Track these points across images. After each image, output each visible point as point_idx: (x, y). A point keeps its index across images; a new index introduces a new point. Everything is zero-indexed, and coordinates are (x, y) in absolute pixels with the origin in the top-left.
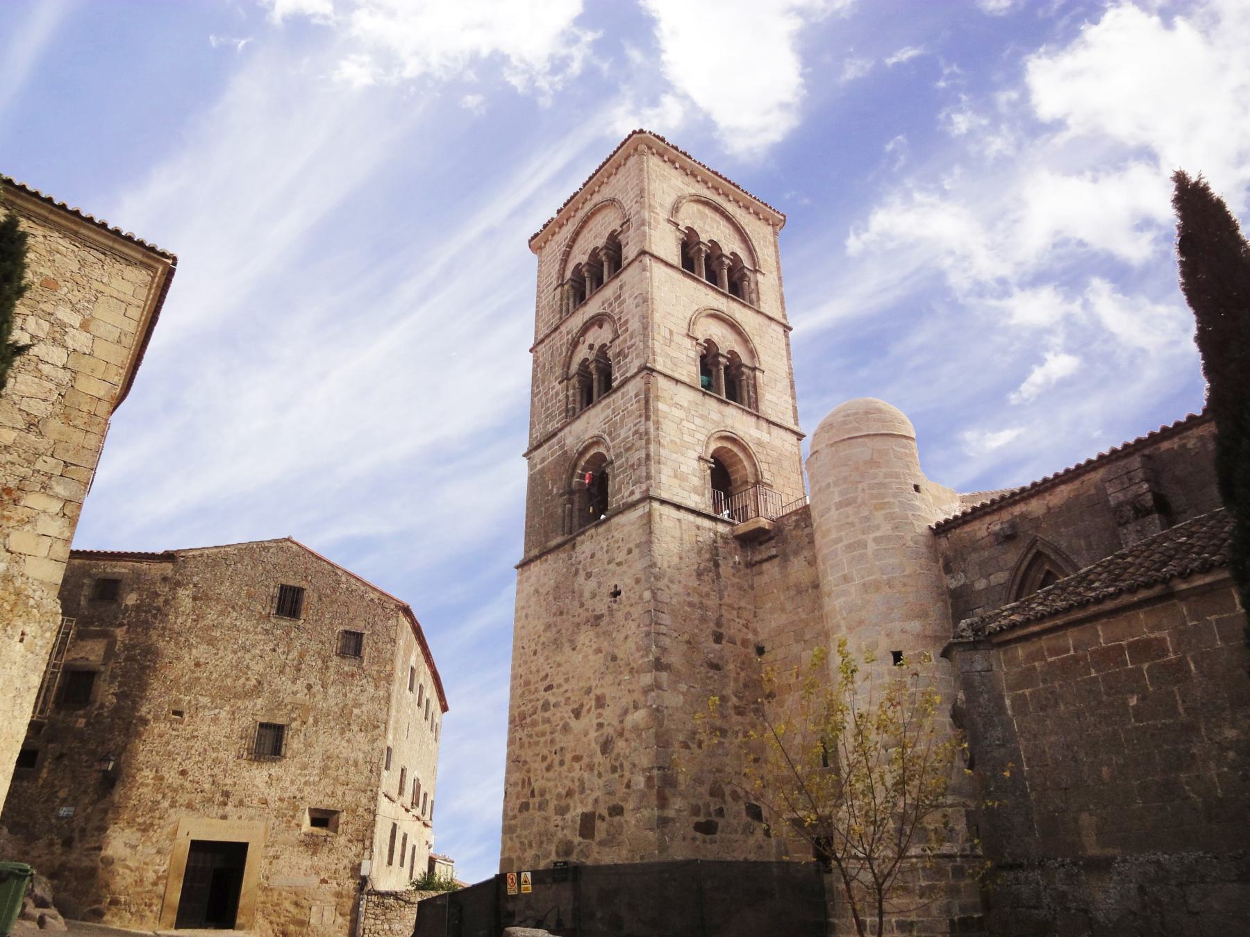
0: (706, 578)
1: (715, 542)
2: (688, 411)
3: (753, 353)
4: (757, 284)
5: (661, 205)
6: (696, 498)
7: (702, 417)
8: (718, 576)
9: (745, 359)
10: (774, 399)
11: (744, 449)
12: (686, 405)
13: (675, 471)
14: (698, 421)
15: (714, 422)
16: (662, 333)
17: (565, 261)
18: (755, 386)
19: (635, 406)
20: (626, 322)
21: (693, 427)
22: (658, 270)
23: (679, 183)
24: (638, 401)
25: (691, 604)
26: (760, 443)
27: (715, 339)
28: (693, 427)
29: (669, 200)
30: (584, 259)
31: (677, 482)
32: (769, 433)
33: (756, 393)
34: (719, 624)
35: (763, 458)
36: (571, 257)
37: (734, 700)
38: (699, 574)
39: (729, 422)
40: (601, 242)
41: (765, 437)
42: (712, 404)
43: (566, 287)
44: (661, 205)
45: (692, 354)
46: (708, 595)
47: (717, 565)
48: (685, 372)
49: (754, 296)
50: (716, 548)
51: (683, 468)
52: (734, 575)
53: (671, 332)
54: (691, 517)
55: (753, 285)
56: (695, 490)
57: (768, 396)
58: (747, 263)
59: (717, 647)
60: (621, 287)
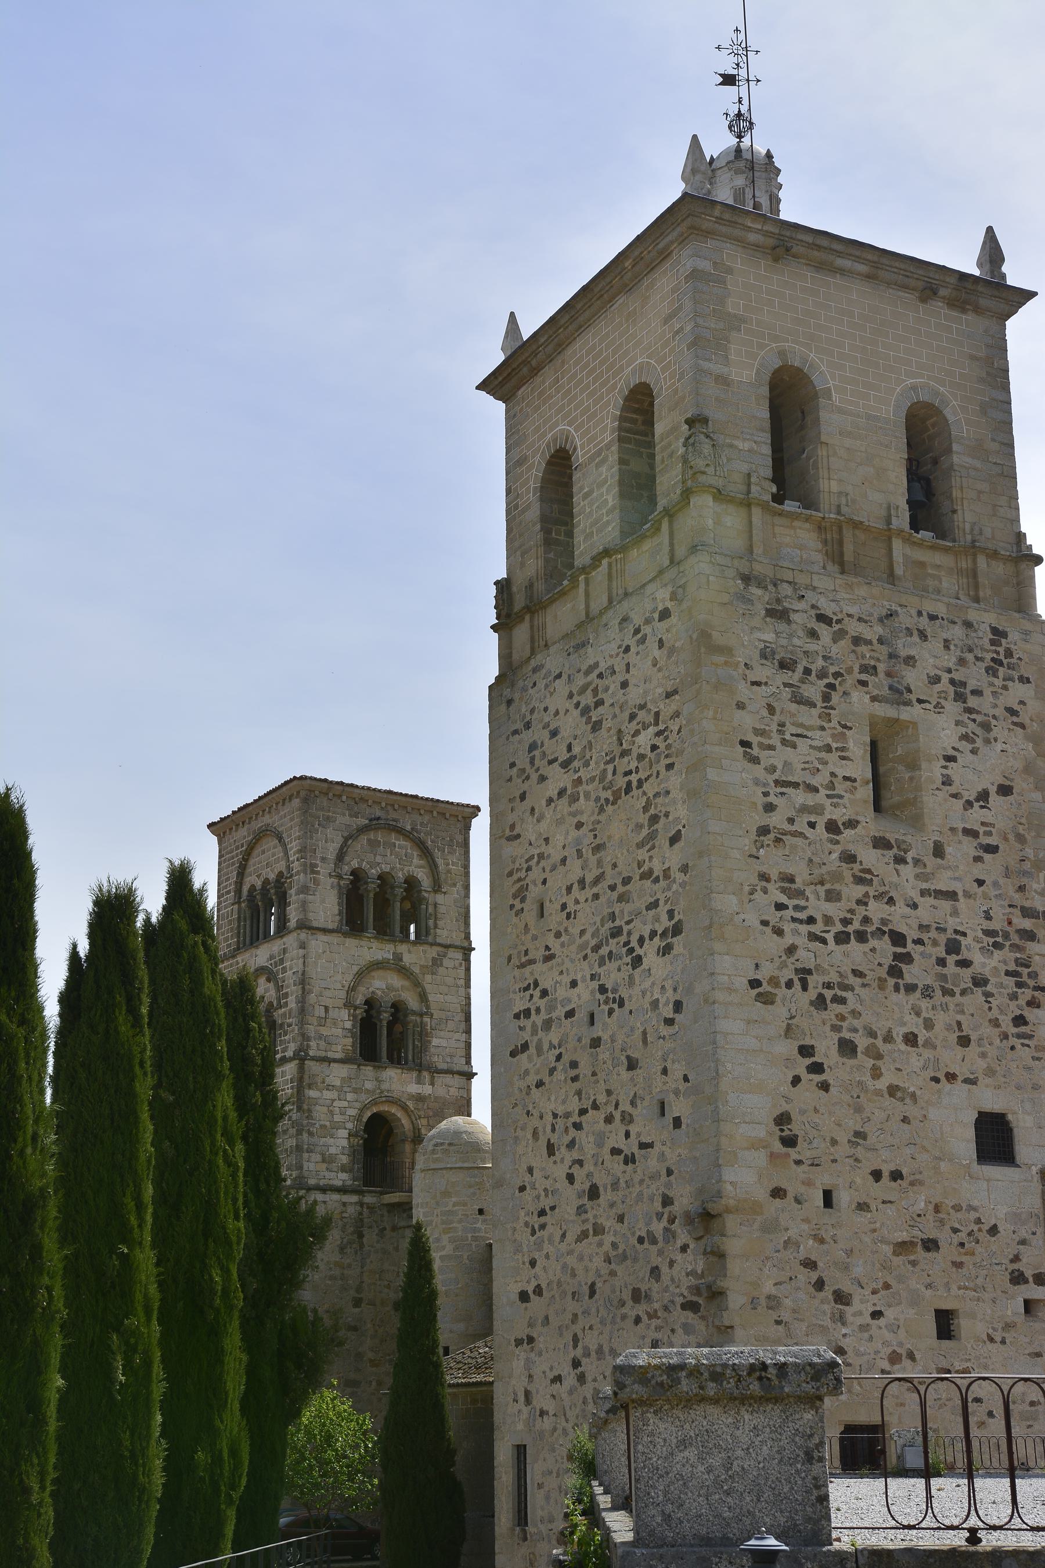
0: (349, 1250)
1: (361, 1214)
2: (340, 1089)
3: (423, 997)
4: (435, 905)
5: (323, 859)
6: (344, 1176)
7: (355, 1091)
8: (362, 1246)
9: (412, 1002)
10: (444, 1043)
11: (404, 1108)
12: (338, 1083)
13: (323, 1155)
14: (350, 1096)
15: (368, 1091)
16: (317, 1014)
17: (241, 875)
18: (421, 1034)
19: (290, 1091)
20: (286, 995)
21: (345, 1104)
22: (318, 943)
23: (347, 819)
24: (292, 1088)
25: (332, 1278)
26: (420, 1098)
28: (345, 1104)
29: (332, 850)
30: (259, 884)
31: (325, 1165)
32: (432, 1084)
34: (359, 1290)
35: (422, 1113)
36: (248, 871)
37: (370, 1355)
38: (342, 1249)
39: (385, 1086)
40: (272, 876)
41: (427, 1090)
42: (368, 1070)
43: (243, 905)
44: (323, 859)
45: (348, 1025)
46: (349, 1266)
47: (361, 1236)
48: (339, 1048)
49: (431, 922)
50: (362, 1220)
51: (333, 1150)
52: (378, 1242)
53: (326, 1008)
54: (336, 1197)
55: (431, 910)
56: (343, 1169)
57: (435, 1042)
58: (426, 883)
59: (357, 1310)
60: (285, 951)
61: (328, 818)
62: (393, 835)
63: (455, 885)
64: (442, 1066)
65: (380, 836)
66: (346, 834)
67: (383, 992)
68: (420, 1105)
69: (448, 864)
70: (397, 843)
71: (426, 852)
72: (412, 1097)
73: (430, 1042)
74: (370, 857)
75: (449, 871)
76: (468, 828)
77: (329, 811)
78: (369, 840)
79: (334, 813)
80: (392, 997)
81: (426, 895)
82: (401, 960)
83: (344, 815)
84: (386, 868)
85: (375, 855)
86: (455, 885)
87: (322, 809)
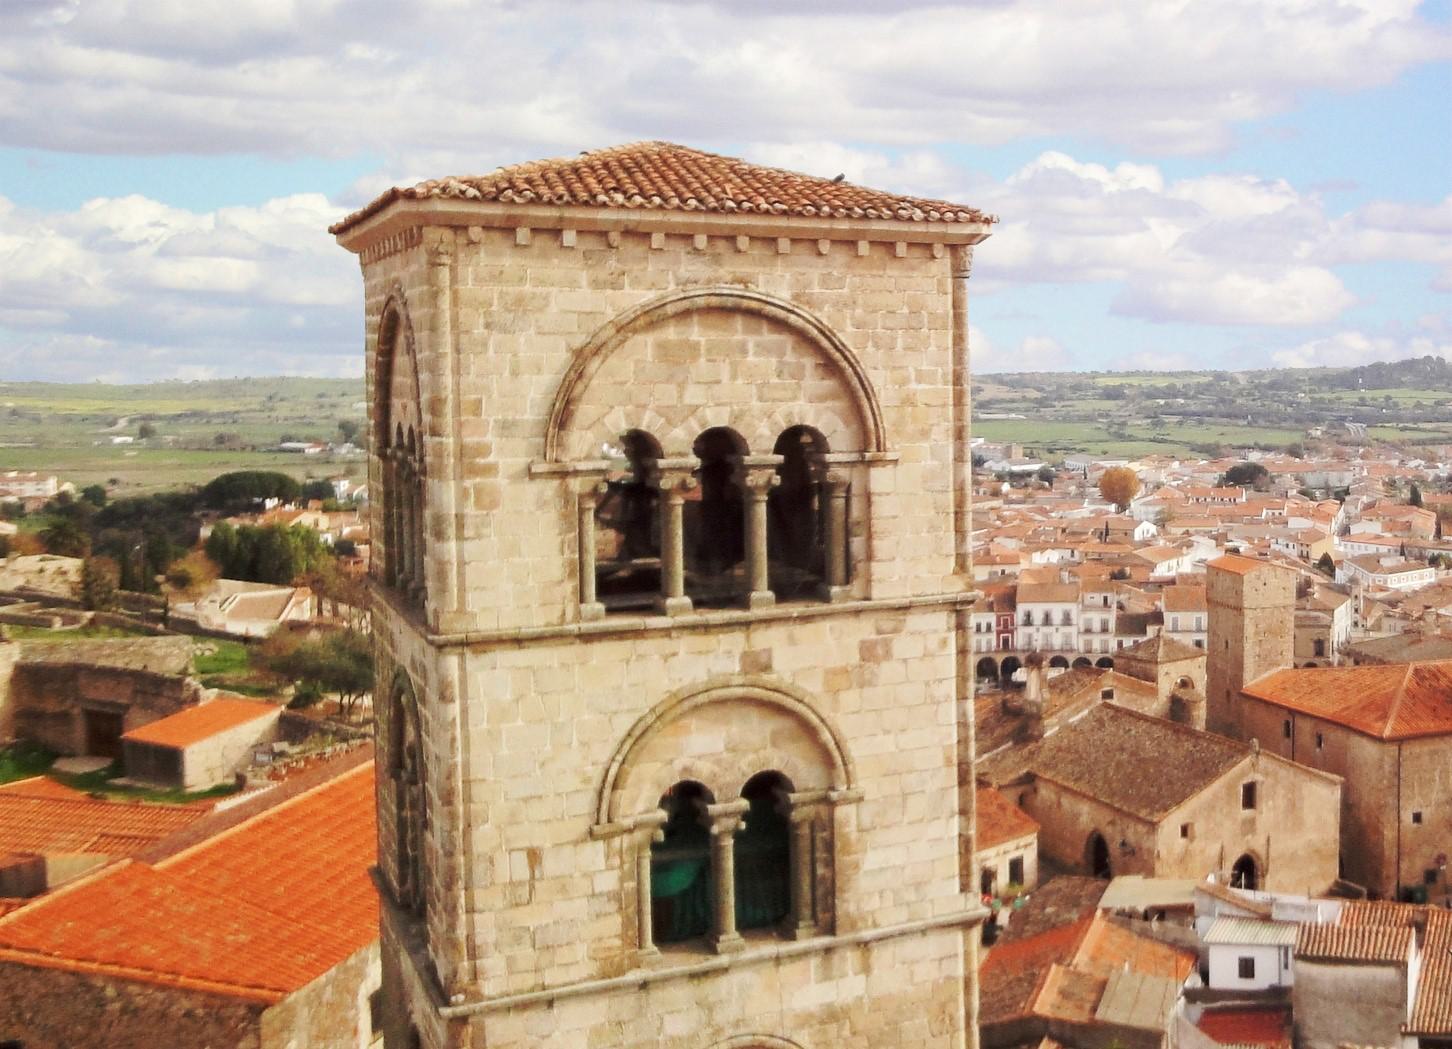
18: (830, 846)
23: (585, 297)
26: (832, 1015)
27: (702, 773)
33: (830, 863)
58: (840, 447)
61: (520, 301)
62: (739, 322)
63: (925, 434)
64: (892, 919)
65: (697, 332)
66: (579, 341)
67: (718, 762)
68: (832, 1028)
69: (904, 382)
70: (751, 341)
71: (833, 363)
72: (805, 1020)
73: (857, 866)
74: (667, 394)
75: (908, 401)
76: (959, 273)
77: (522, 280)
78: (663, 348)
79: (541, 282)
80: (748, 768)
81: (842, 473)
82: (767, 668)
83: (573, 284)
84: (718, 419)
85: (682, 386)
86: (925, 434)
87: (498, 277)
